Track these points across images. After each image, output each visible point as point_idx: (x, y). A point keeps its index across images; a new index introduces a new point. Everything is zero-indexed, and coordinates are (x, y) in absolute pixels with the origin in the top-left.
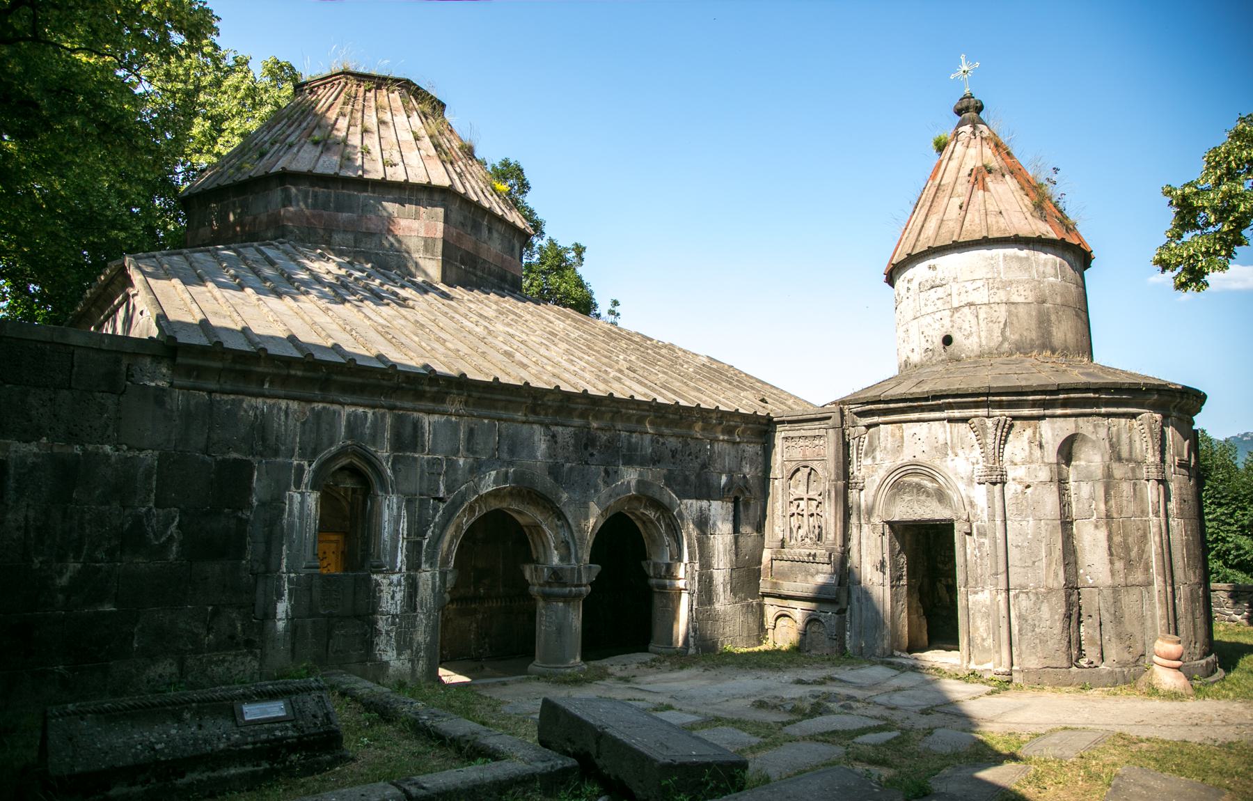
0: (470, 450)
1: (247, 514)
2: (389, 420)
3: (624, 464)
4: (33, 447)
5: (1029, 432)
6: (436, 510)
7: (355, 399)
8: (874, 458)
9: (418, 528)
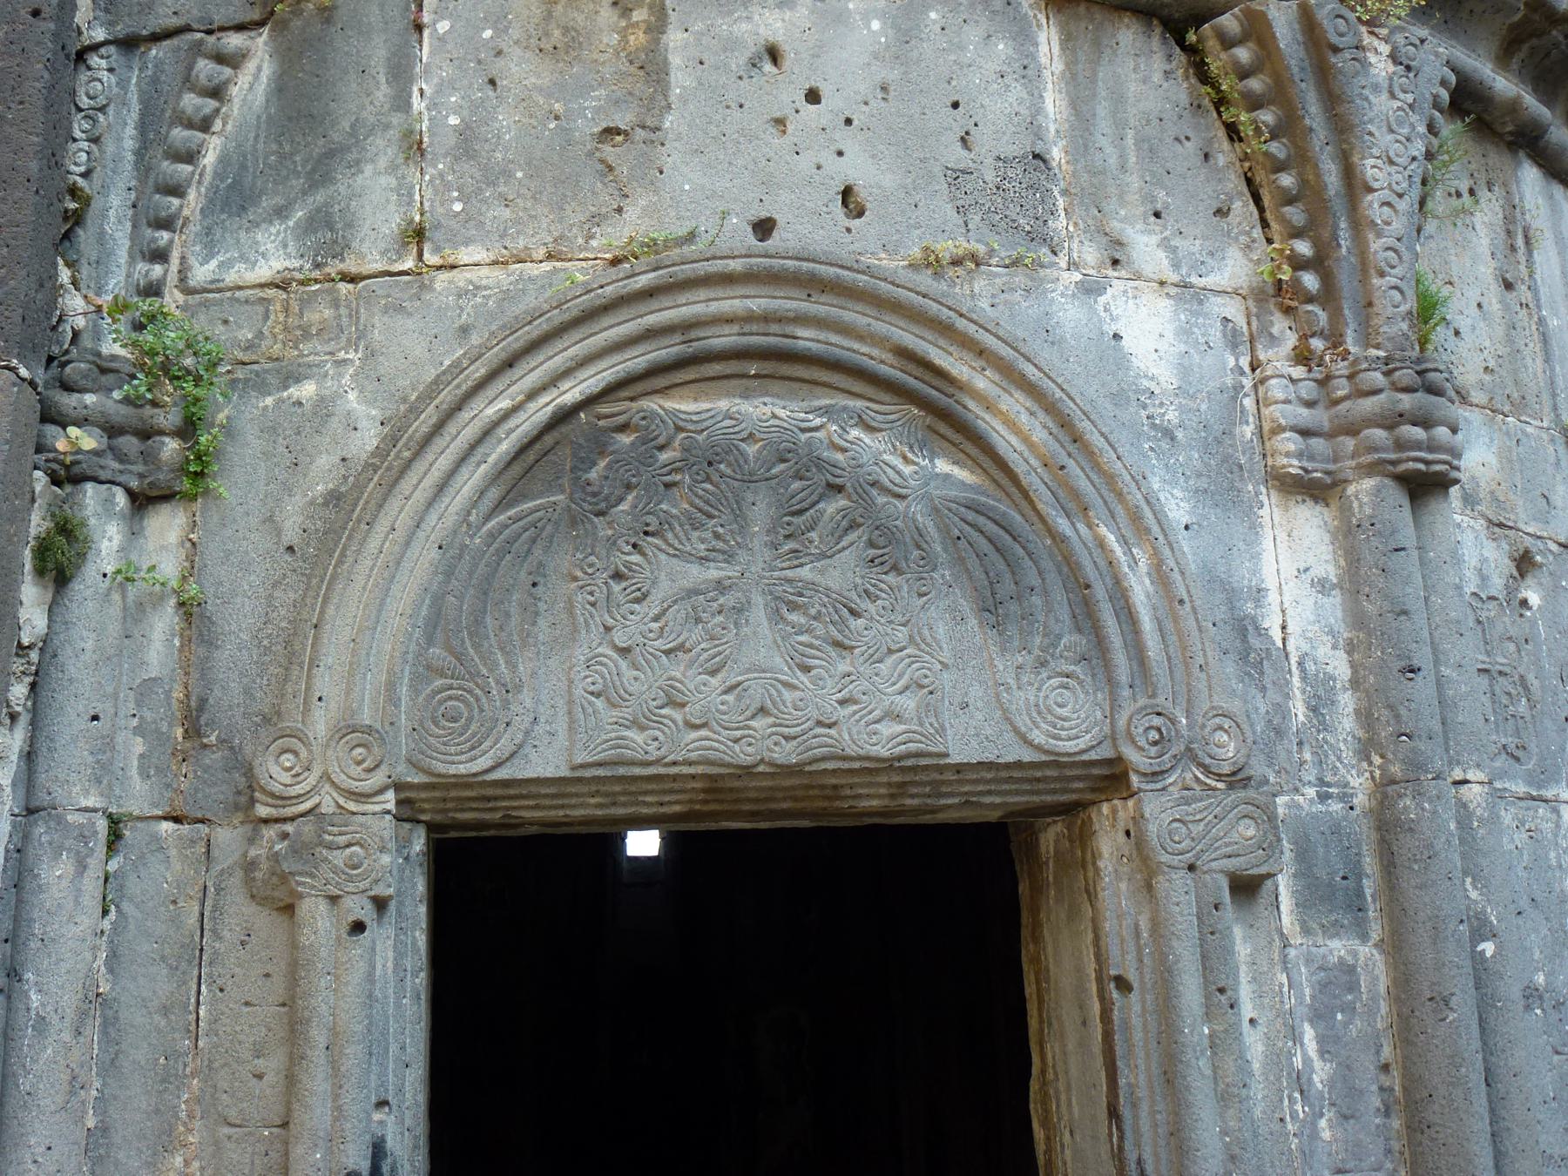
5: (1487, 215)
8: (327, 234)
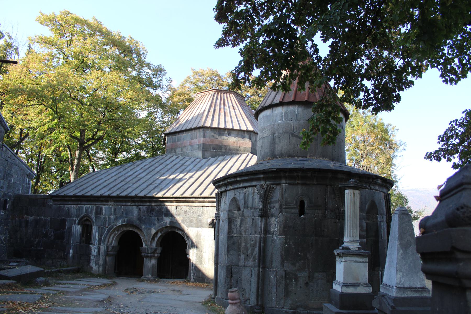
0: (115, 214)
1: (65, 230)
2: (94, 208)
3: (165, 216)
4: (32, 218)
6: (105, 230)
7: (87, 203)
9: (101, 235)
